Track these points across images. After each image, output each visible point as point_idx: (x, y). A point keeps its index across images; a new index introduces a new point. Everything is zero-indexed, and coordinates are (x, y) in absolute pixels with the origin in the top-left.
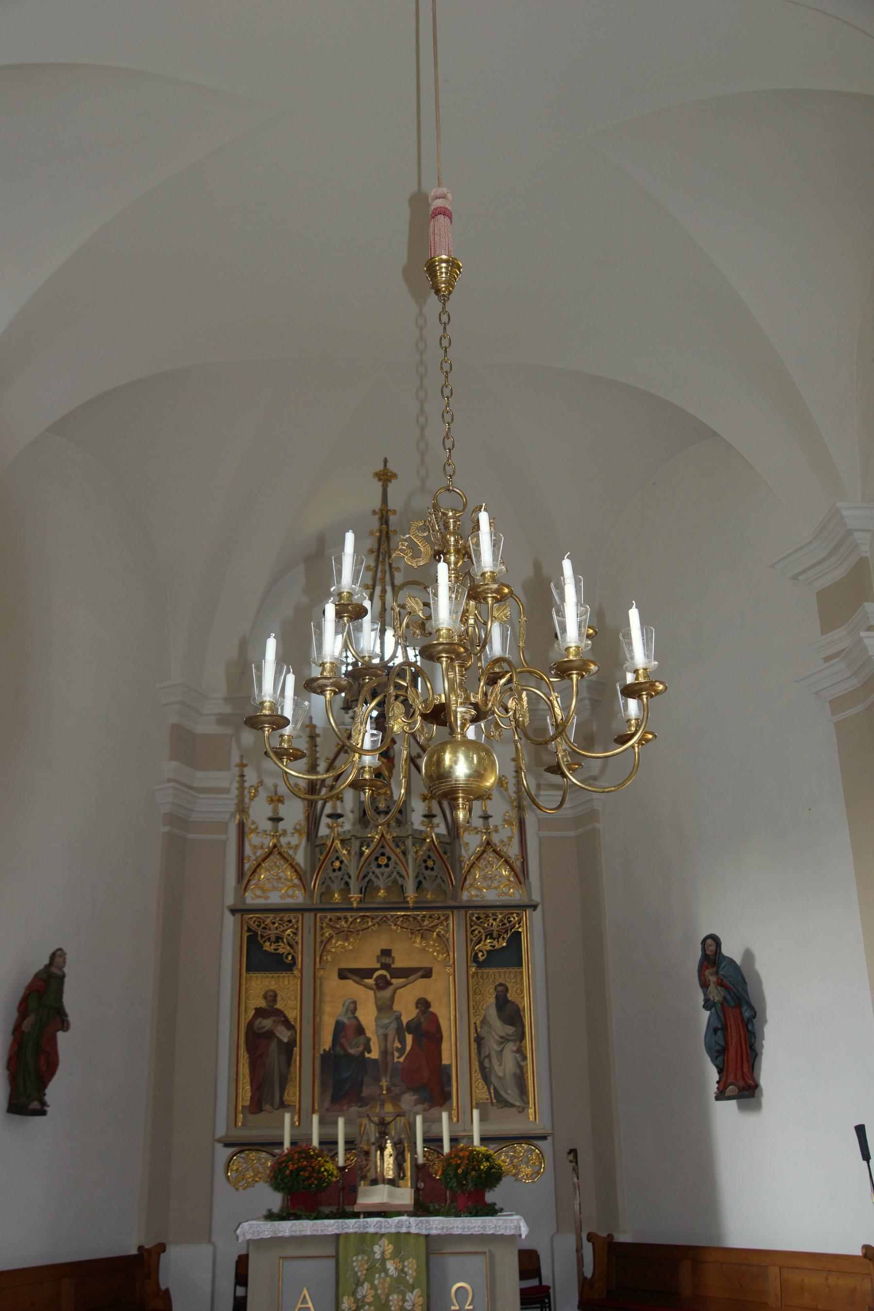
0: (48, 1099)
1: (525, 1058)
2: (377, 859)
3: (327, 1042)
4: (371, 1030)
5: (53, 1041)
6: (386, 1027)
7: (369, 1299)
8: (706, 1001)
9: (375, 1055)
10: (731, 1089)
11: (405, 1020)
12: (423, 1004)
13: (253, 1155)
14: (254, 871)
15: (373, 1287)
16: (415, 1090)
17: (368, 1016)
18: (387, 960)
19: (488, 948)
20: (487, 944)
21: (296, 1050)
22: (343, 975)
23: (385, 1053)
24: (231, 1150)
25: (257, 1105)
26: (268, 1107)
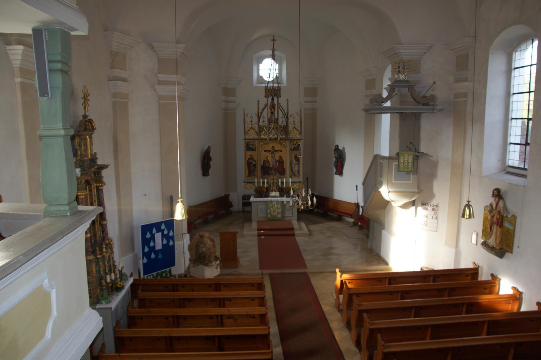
3: (262, 164)
4: (270, 162)
6: (273, 161)
7: (272, 210)
8: (335, 156)
9: (271, 166)
10: (338, 173)
11: (277, 160)
12: (280, 157)
13: (249, 184)
14: (247, 132)
17: (270, 159)
18: (273, 148)
19: (293, 147)
20: (293, 147)
22: (265, 151)
23: (273, 166)
24: (246, 184)
25: (249, 175)
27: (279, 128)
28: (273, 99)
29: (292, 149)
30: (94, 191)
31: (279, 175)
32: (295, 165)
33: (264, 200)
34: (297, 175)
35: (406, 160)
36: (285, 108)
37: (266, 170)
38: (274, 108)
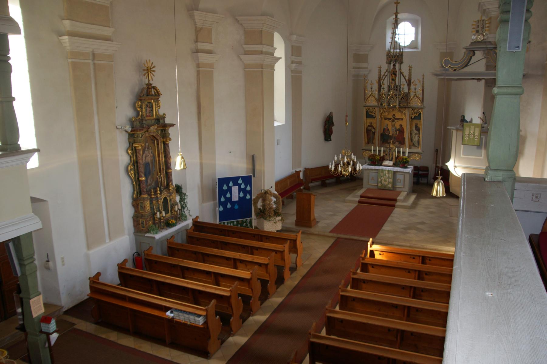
0: (331, 138)
1: (419, 138)
2: (391, 98)
4: (390, 130)
5: (332, 128)
6: (393, 129)
11: (397, 128)
12: (401, 126)
13: (367, 152)
15: (384, 178)
16: (398, 142)
17: (390, 127)
21: (376, 133)
23: (393, 134)
26: (370, 143)
27: (398, 95)
28: (394, 65)
29: (413, 118)
30: (161, 145)
31: (399, 144)
32: (415, 135)
33: (375, 169)
34: (417, 146)
35: (472, 132)
36: (406, 74)
37: (385, 139)
38: (395, 75)
